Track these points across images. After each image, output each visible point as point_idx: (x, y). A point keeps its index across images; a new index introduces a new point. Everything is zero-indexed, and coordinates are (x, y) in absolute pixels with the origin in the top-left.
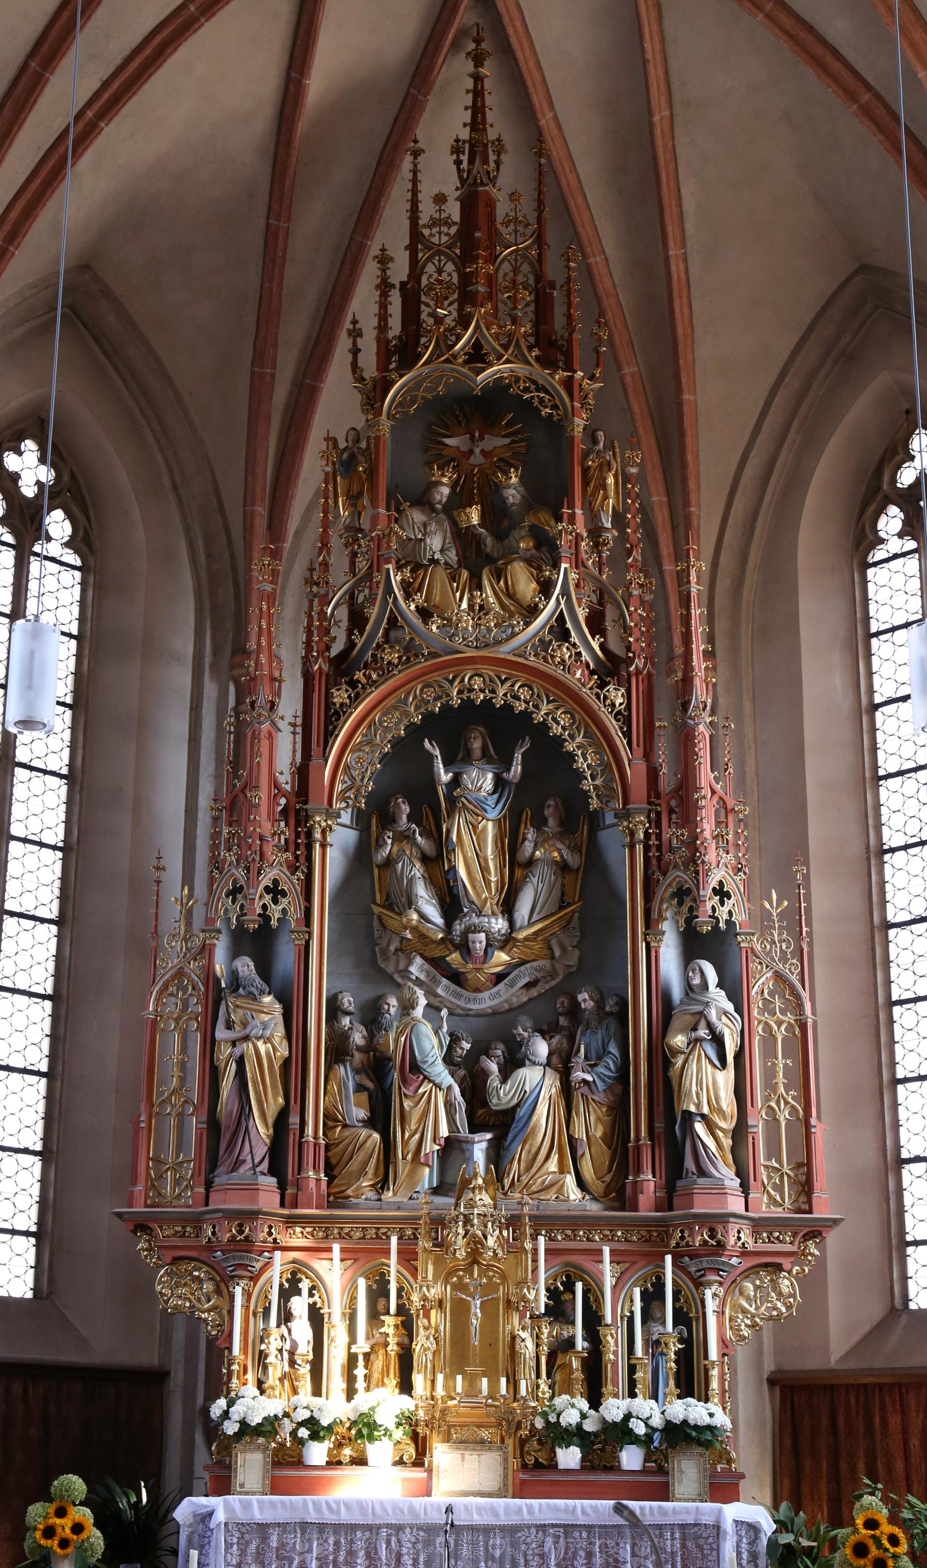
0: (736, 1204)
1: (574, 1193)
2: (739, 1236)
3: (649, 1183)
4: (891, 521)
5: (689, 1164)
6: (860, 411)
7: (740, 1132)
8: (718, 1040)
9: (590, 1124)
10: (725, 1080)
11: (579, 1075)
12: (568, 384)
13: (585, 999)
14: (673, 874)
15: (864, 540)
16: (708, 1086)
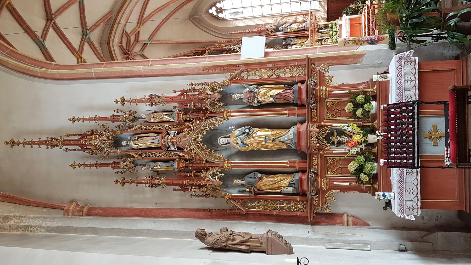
0: (308, 22)
1: (307, 42)
2: (312, 21)
3: (306, 33)
4: (220, 15)
5: (303, 28)
6: (207, 19)
7: (300, 22)
8: (289, 25)
9: (299, 41)
10: (293, 25)
11: (293, 43)
12: (207, 50)
13: (284, 43)
14: (269, 32)
15: (223, 19)
16: (294, 27)
